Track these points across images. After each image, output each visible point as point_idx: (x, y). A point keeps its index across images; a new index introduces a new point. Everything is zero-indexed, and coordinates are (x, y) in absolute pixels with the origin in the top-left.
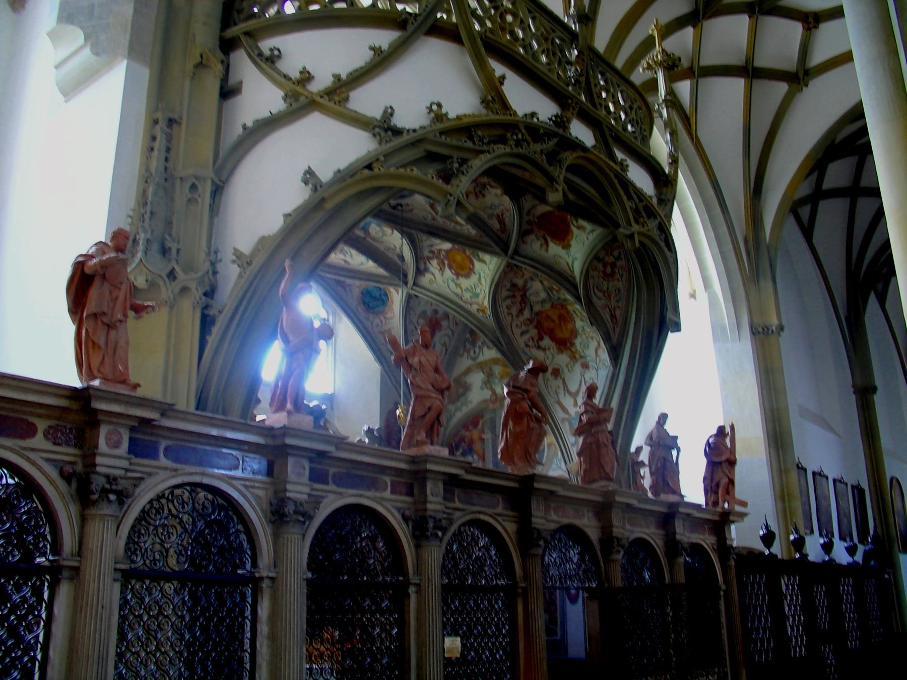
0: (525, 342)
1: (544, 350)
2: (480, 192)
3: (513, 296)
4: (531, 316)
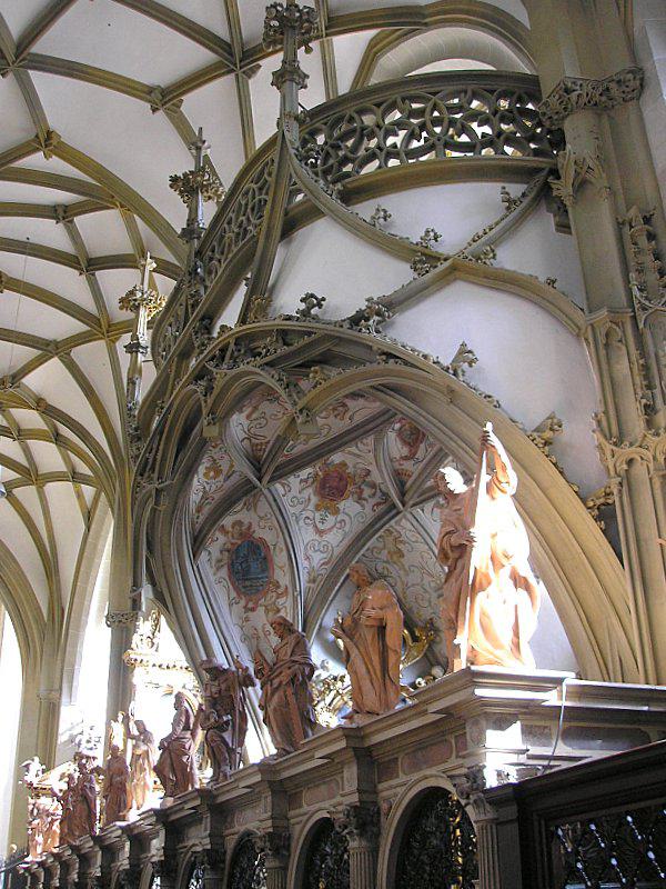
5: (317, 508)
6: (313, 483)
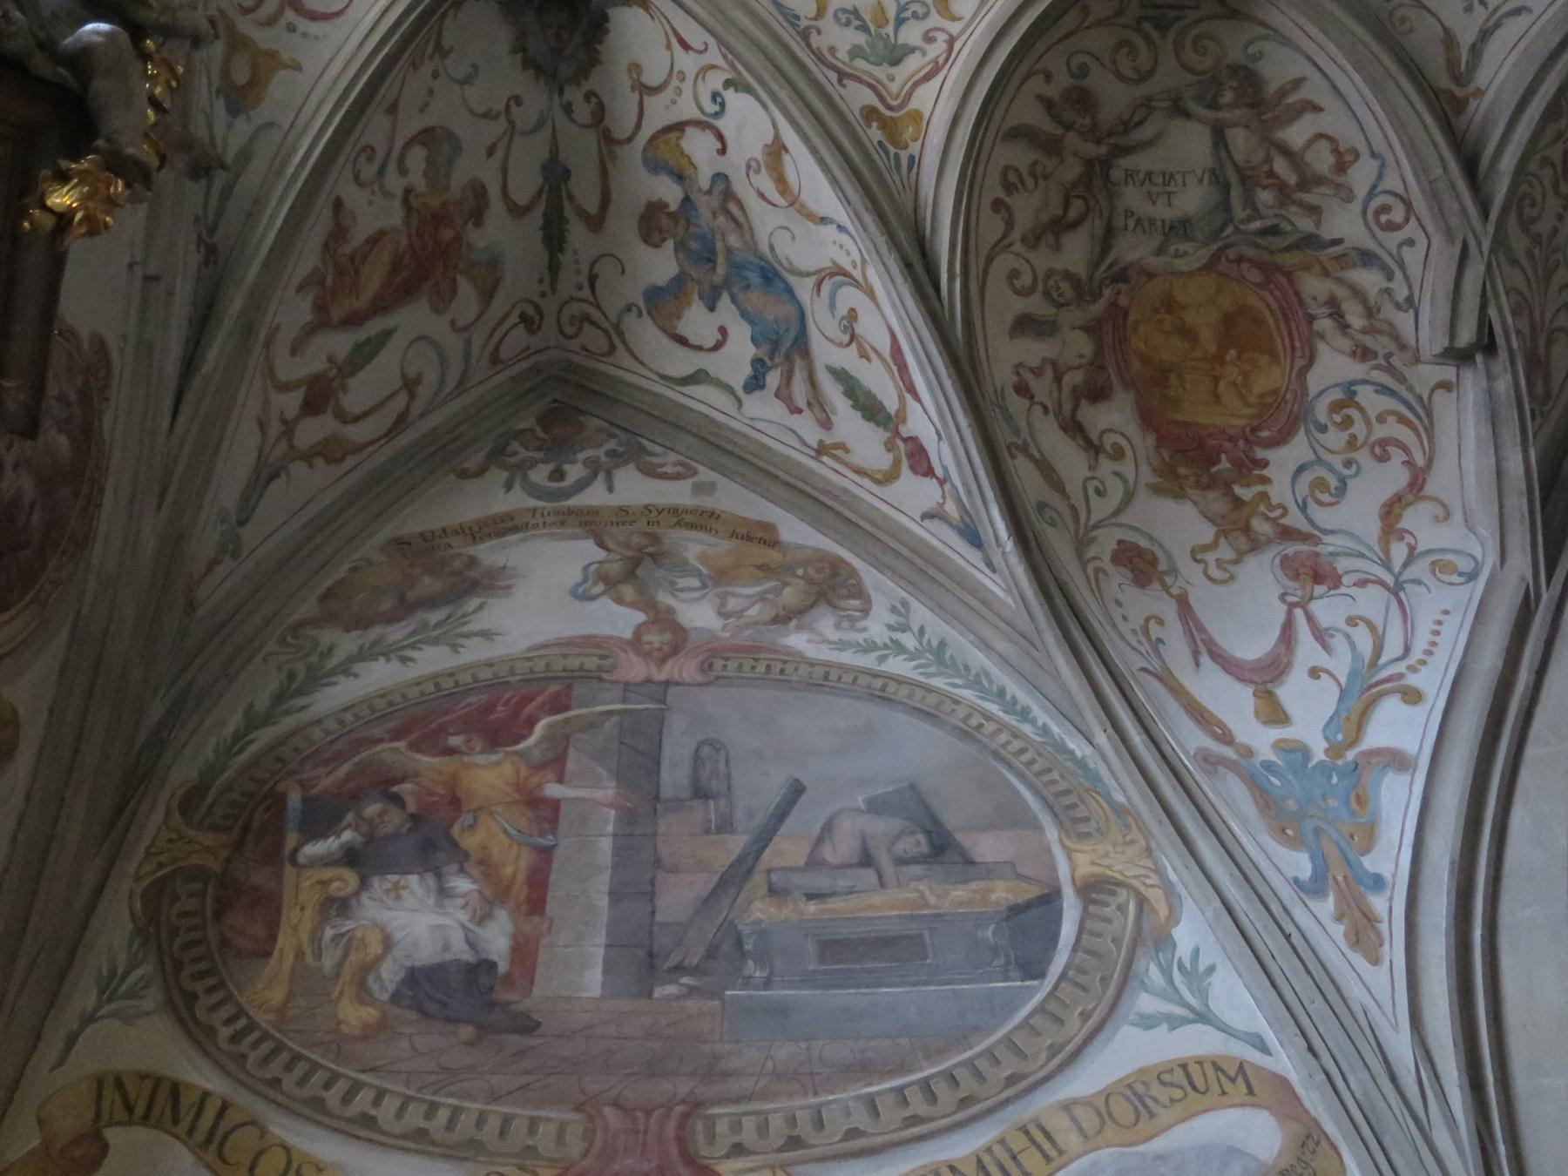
0: (1018, 368)
1: (1093, 448)
3: (1052, 147)
4: (1091, 277)
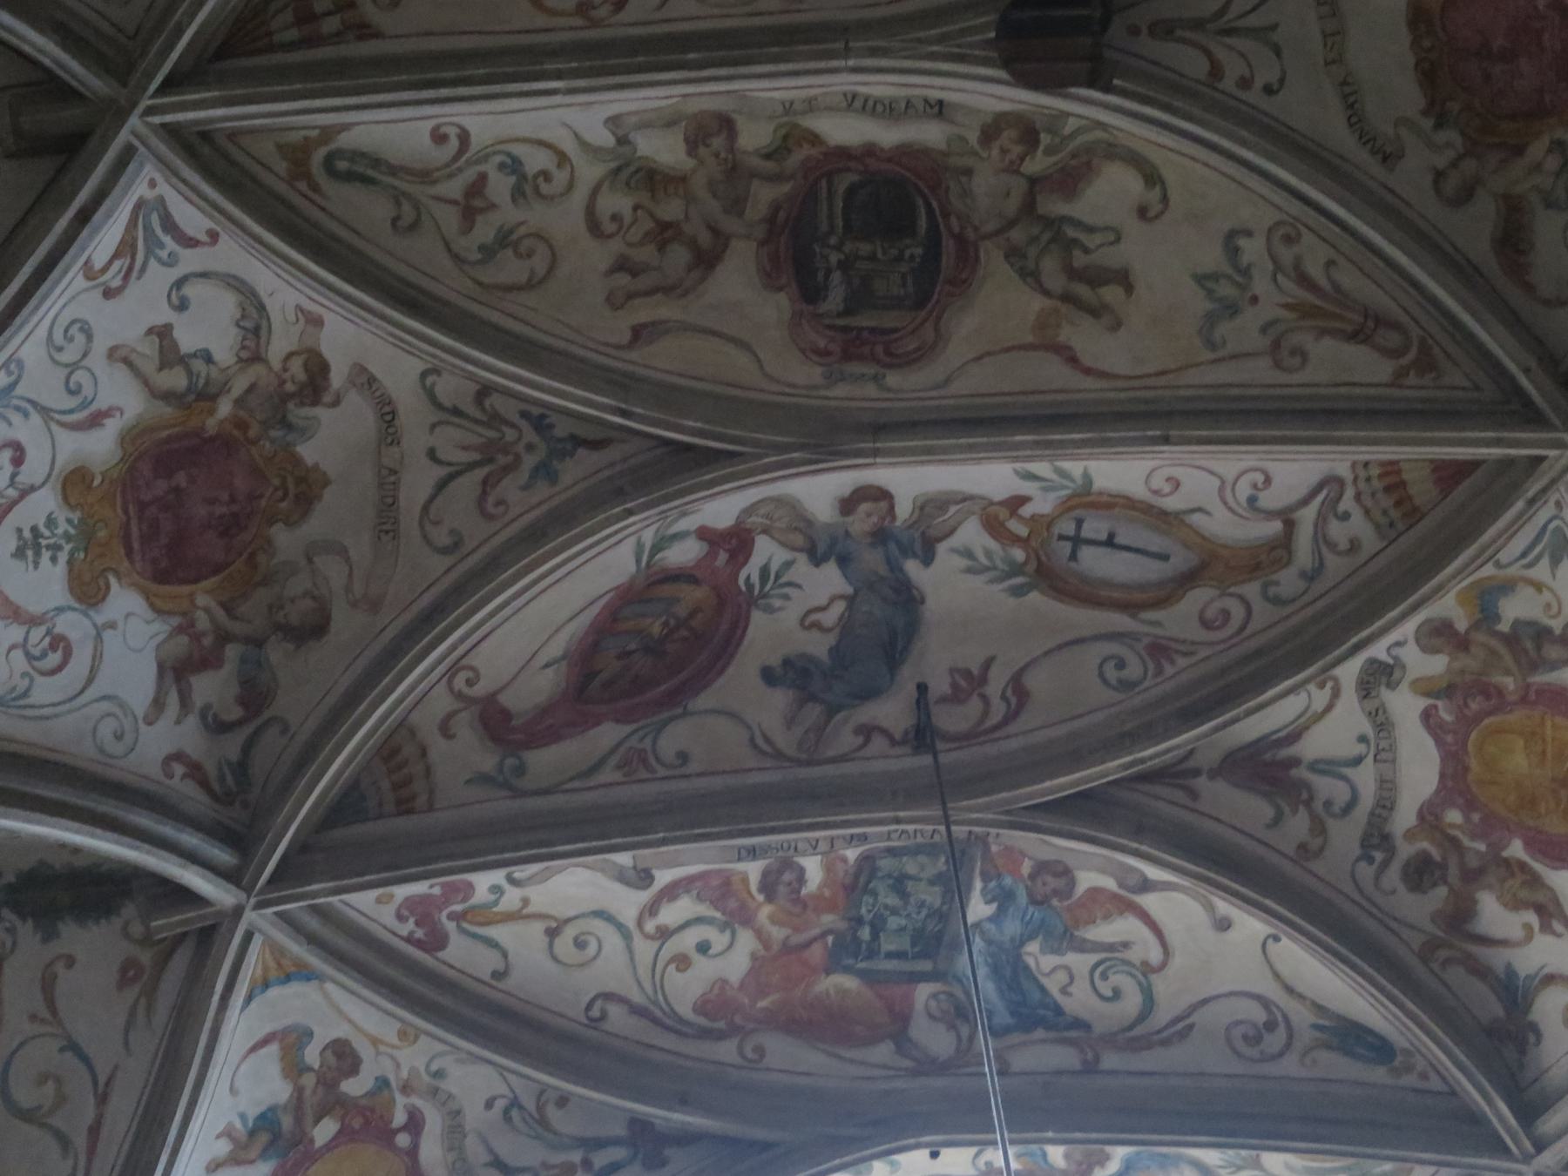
2: (1073, 273)
5: (75, 482)
6: (167, 396)
